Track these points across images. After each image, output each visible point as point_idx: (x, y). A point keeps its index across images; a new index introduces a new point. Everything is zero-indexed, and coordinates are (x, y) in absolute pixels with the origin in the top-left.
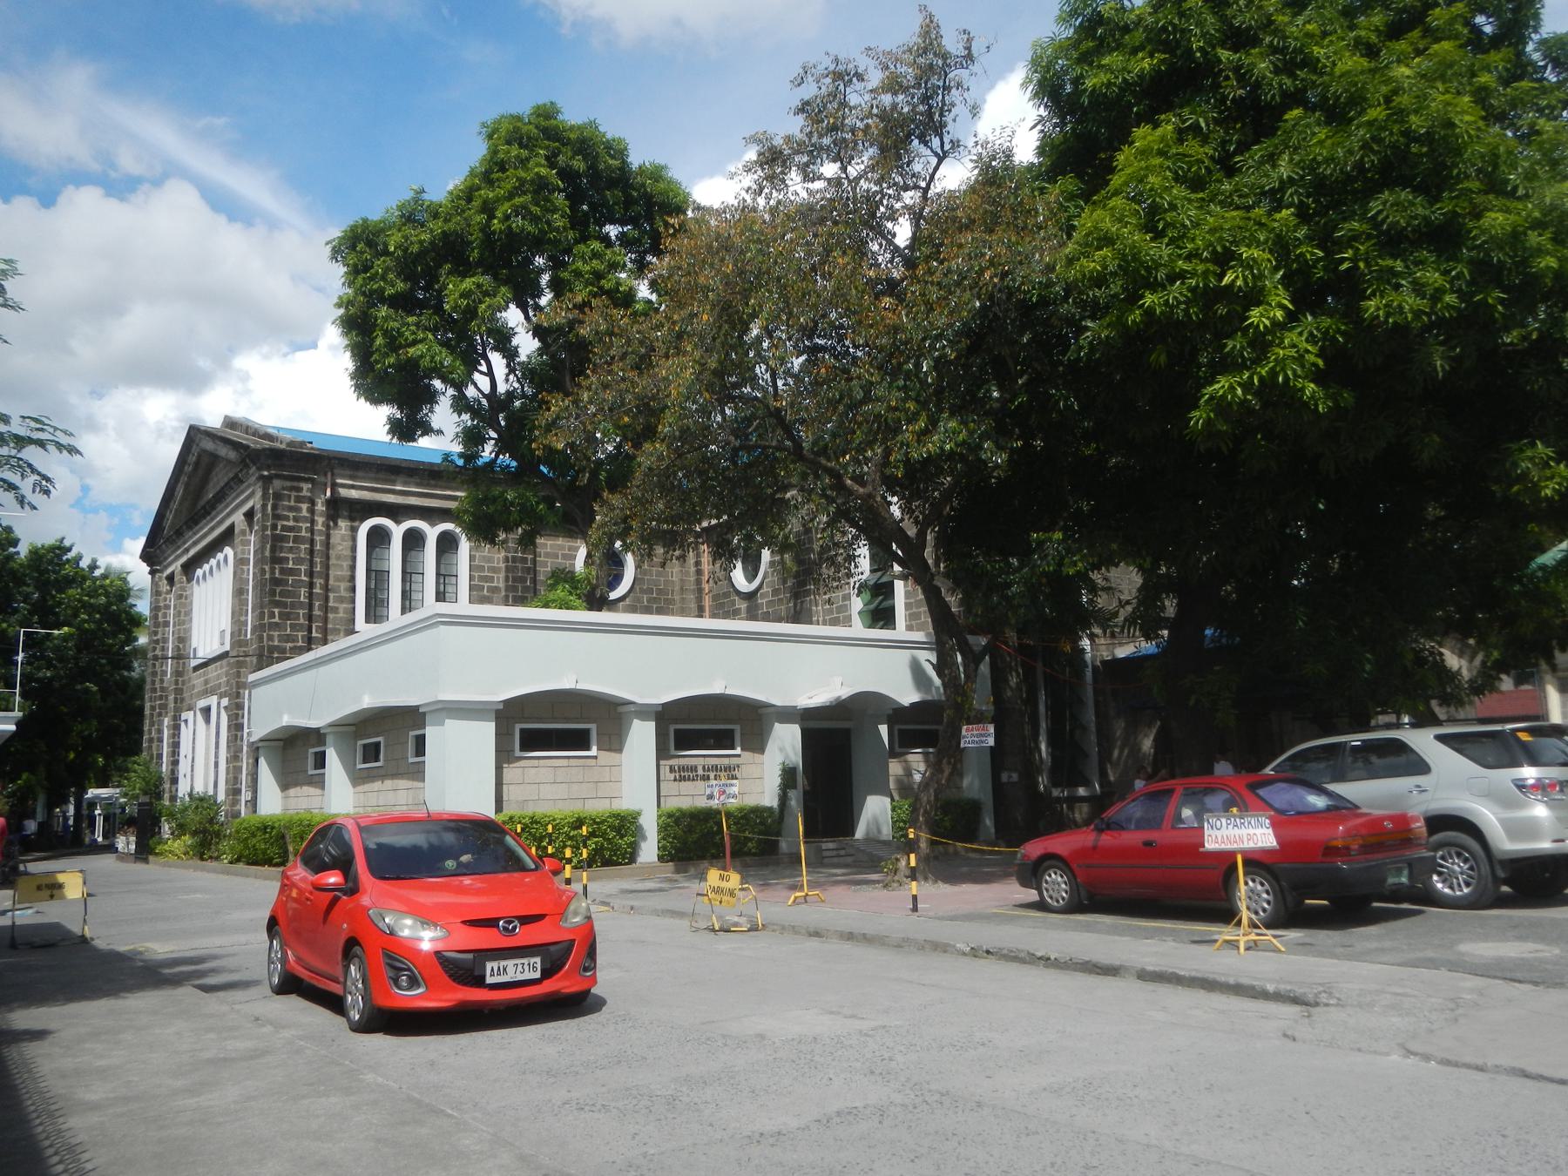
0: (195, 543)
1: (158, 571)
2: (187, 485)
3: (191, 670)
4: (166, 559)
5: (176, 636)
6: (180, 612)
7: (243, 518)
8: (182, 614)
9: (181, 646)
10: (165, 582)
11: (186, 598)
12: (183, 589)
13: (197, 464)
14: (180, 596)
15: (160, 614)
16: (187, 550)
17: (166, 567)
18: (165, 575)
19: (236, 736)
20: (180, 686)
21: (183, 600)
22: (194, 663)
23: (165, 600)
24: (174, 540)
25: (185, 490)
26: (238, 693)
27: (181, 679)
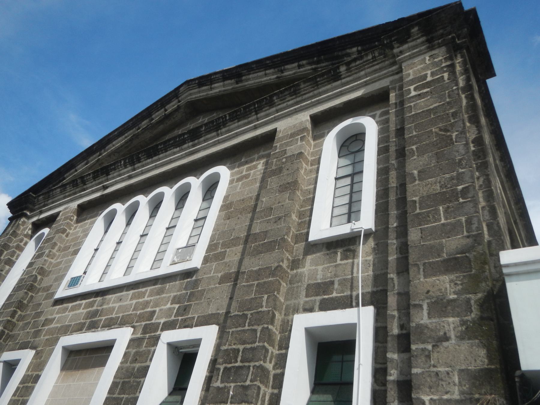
0: (130, 177)
1: (26, 216)
2: (136, 136)
3: (52, 300)
4: (44, 206)
5: (36, 266)
6: (55, 244)
7: (309, 118)
8: (57, 248)
9: (39, 277)
10: (30, 226)
11: (67, 236)
12: (69, 226)
13: (167, 117)
14: (64, 231)
15: (5, 252)
16: (105, 188)
17: (41, 212)
18: (35, 219)
19: (259, 388)
20: (14, 320)
21: (64, 236)
22: (61, 292)
23: (21, 240)
24: (84, 183)
25: (126, 142)
26: (274, 316)
27: (19, 313)
